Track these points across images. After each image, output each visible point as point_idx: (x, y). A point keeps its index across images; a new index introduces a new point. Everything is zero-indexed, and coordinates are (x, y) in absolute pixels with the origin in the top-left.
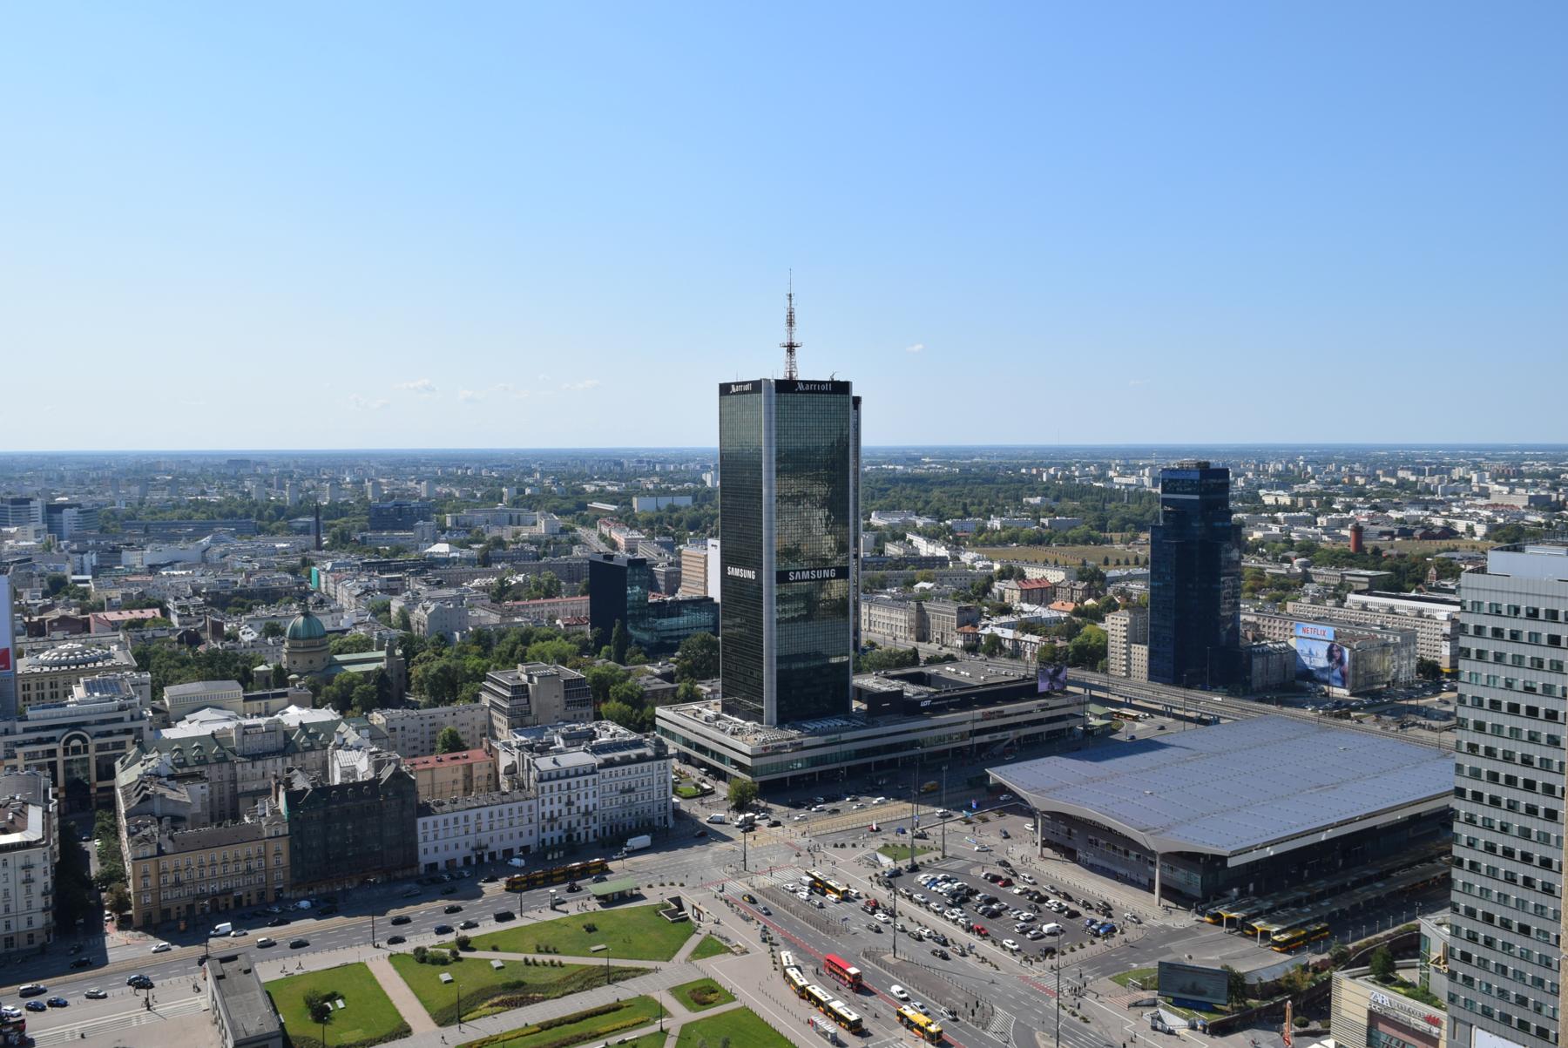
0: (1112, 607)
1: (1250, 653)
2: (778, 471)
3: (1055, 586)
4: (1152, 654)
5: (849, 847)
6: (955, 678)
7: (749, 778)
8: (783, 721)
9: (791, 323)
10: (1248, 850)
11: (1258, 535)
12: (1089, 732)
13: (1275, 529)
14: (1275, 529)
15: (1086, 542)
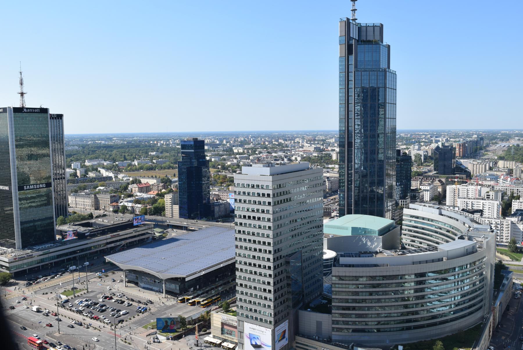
0: (171, 191)
1: (214, 205)
2: (17, 146)
3: (153, 185)
4: (180, 208)
5: (49, 294)
6: (102, 223)
7: (8, 272)
8: (24, 246)
9: (22, 84)
10: (195, 273)
11: (229, 163)
12: (154, 239)
13: (235, 161)
14: (235, 161)
15: (169, 168)
